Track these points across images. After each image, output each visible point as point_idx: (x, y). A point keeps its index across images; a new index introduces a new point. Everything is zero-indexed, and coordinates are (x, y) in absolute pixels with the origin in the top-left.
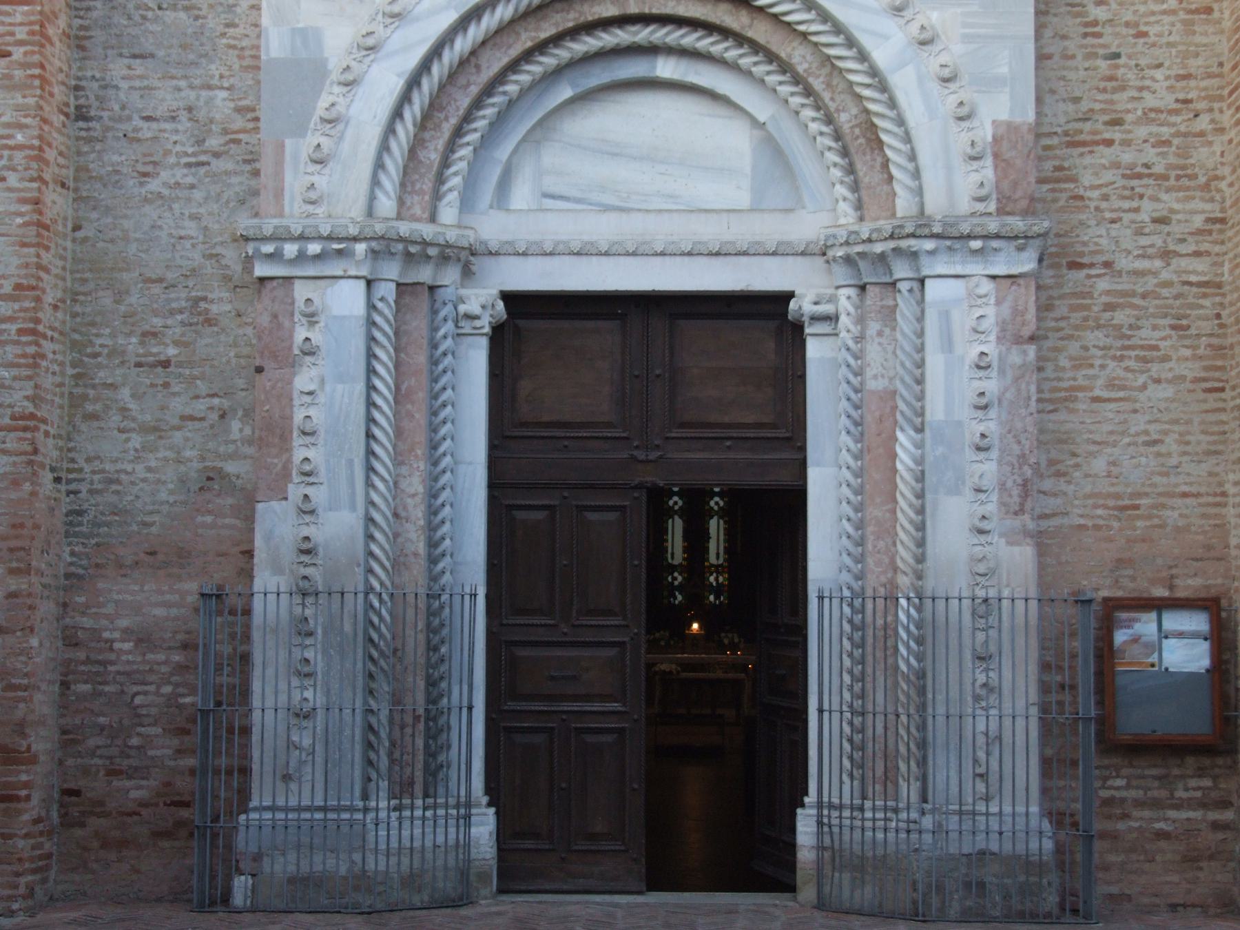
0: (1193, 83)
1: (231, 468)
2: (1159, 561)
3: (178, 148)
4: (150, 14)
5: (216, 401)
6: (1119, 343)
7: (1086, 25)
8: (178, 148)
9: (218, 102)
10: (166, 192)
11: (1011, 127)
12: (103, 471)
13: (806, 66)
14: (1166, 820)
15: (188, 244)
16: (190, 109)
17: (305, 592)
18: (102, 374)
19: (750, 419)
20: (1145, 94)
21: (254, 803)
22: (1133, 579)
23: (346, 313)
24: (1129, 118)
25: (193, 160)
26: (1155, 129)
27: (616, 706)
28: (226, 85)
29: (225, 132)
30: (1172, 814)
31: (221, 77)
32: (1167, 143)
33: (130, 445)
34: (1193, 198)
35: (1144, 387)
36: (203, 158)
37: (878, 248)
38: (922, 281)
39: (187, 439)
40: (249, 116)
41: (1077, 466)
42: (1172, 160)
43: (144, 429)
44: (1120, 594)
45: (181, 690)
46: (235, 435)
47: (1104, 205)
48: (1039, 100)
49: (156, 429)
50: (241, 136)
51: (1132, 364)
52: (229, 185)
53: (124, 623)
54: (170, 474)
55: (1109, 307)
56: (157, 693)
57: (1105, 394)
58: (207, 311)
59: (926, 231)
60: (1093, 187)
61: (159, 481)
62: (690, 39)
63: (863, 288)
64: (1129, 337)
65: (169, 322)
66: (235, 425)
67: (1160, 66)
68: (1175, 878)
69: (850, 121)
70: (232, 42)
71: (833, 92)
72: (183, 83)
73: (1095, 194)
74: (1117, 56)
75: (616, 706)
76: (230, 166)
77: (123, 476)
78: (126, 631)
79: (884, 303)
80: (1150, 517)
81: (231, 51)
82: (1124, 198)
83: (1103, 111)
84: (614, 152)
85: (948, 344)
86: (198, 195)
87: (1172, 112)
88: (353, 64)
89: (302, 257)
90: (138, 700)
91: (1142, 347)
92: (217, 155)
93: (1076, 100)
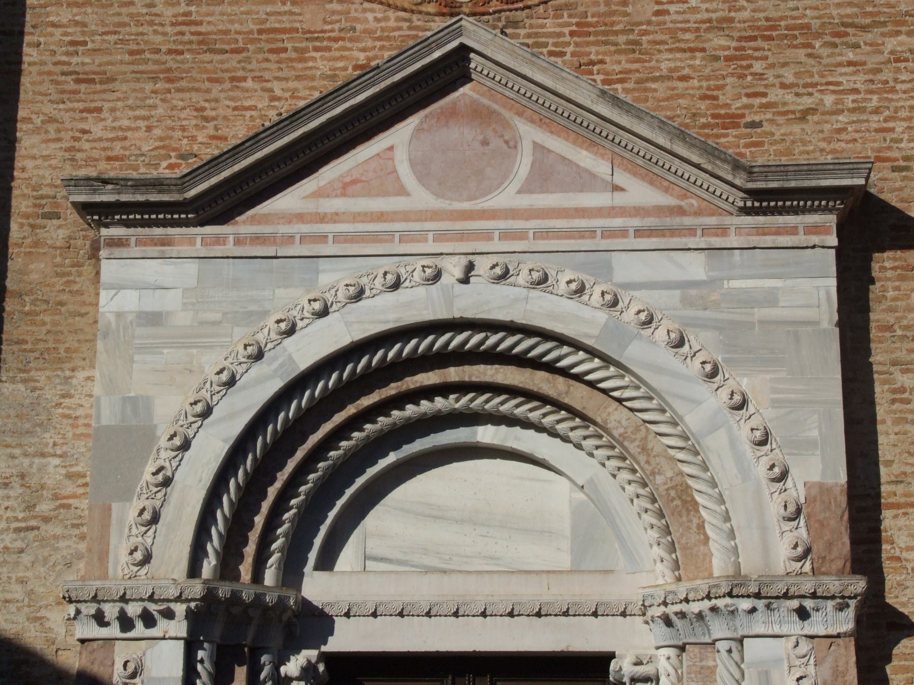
3: (9, 514)
7: (894, 391)
8: (9, 514)
9: (51, 469)
13: (621, 430)
15: (12, 607)
16: (22, 476)
23: (167, 675)
25: (23, 525)
28: (59, 452)
31: (55, 444)
36: (33, 523)
37: (695, 607)
38: (740, 641)
40: (81, 481)
50: (71, 501)
52: (57, 549)
59: (743, 591)
62: (509, 406)
63: (682, 648)
69: (665, 484)
70: (67, 412)
71: (649, 455)
72: (17, 451)
76: (58, 531)
79: (704, 663)
81: (65, 421)
84: (436, 515)
86: (26, 559)
92: (46, 520)
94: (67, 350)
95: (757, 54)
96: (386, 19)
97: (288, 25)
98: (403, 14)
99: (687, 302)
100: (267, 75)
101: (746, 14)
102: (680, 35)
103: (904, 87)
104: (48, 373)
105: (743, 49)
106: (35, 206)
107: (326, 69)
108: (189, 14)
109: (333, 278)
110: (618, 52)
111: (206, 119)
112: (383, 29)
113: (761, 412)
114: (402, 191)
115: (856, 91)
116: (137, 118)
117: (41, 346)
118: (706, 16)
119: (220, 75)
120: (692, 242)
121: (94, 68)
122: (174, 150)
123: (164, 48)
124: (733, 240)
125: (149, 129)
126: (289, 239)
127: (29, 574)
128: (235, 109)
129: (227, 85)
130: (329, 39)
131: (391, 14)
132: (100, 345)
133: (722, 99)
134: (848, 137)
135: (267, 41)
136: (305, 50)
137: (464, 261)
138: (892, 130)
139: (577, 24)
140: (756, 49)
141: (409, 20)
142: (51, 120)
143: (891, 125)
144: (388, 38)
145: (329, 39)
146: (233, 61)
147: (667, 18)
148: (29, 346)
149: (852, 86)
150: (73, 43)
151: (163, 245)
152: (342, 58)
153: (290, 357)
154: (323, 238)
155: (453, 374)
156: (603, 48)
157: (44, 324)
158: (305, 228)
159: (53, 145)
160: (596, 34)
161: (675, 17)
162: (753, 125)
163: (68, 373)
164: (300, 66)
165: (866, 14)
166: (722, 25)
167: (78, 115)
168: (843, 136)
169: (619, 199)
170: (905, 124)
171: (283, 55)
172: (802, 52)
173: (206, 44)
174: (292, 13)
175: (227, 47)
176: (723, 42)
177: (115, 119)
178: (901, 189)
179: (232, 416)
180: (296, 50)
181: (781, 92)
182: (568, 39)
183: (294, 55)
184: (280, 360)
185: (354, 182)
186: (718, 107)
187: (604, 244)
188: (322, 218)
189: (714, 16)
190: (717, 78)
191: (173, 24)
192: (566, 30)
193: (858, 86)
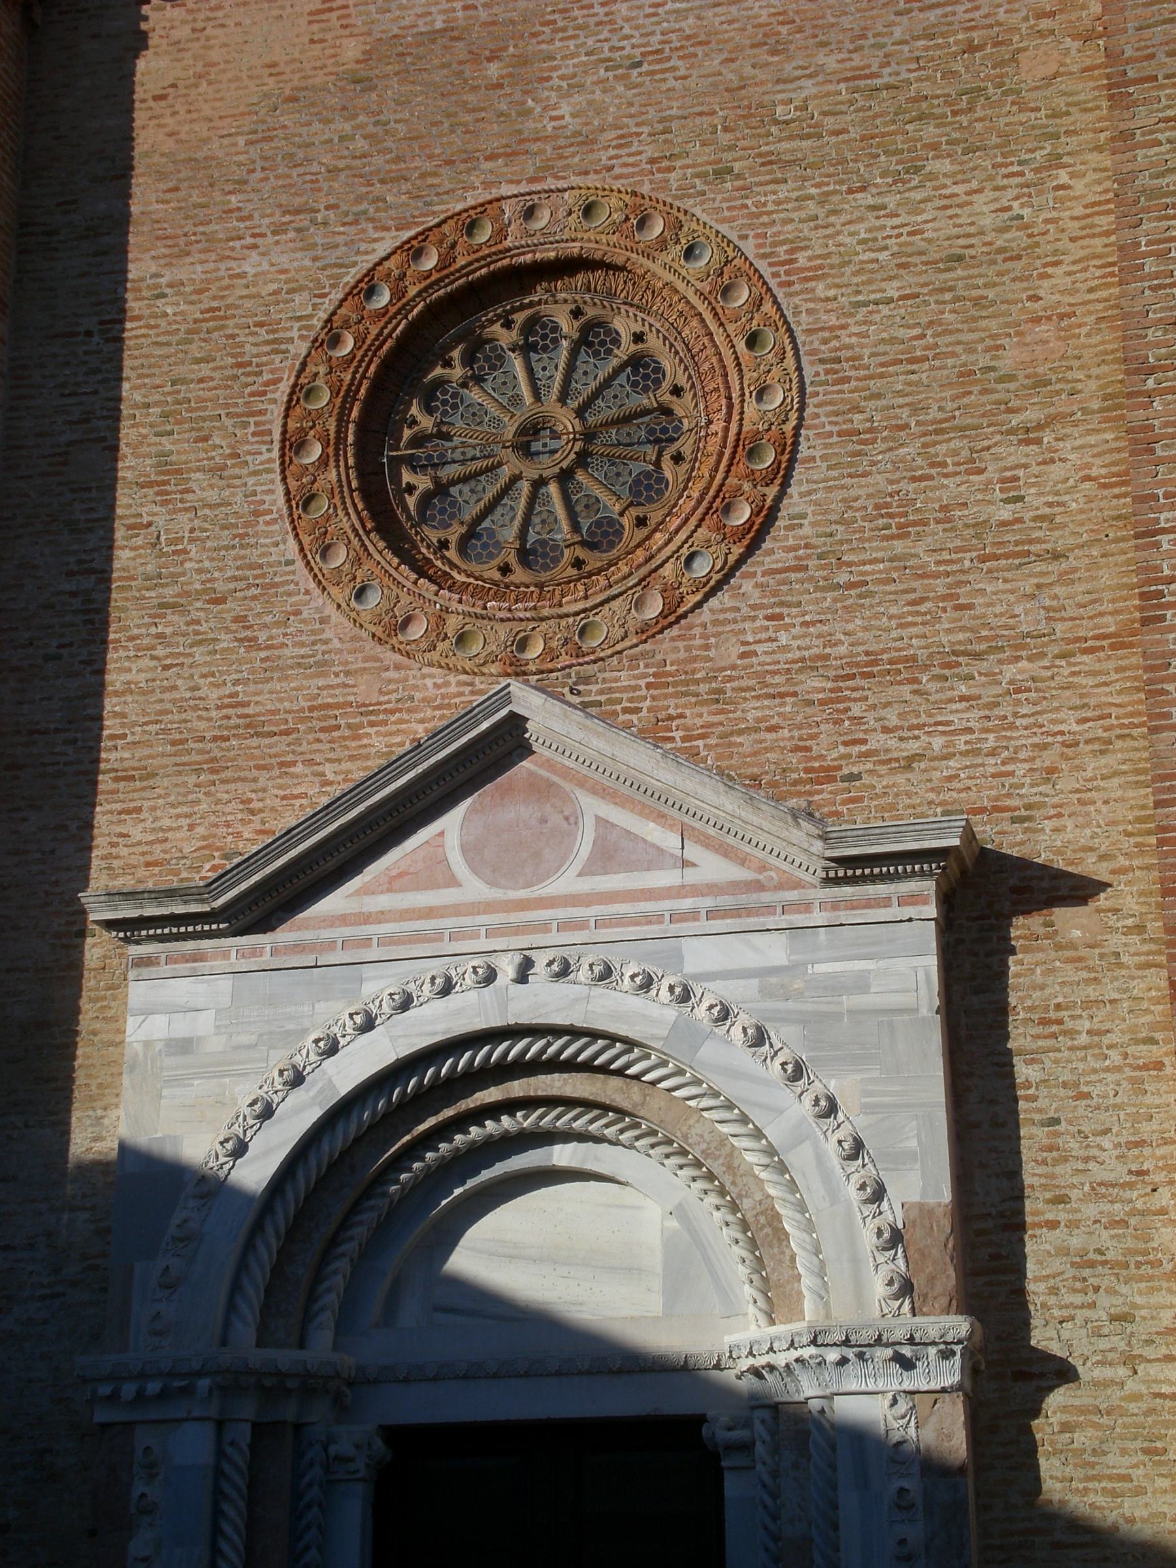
0: (1147, 1151)
6: (1080, 1473)
11: (924, 1212)
20: (1092, 1165)
24: (1074, 1194)
25: (48, 1291)
26: (1107, 1207)
32: (1124, 1223)
34: (1159, 1289)
42: (1130, 1243)
47: (1052, 1300)
55: (1066, 1427)
64: (1092, 1465)
67: (1108, 1131)
71: (735, 1175)
74: (1057, 1121)
82: (1075, 1291)
83: (1044, 1187)
89: (140, 1397)
94: (100, 1086)
95: (855, 695)
96: (447, 684)
98: (464, 677)
99: (766, 992)
100: (318, 758)
101: (843, 649)
102: (769, 679)
103: (1025, 722)
105: (840, 690)
107: (381, 743)
108: (236, 694)
109: (378, 986)
110: (702, 703)
111: (252, 812)
112: (443, 697)
113: (854, 1117)
114: (453, 881)
115: (969, 730)
116: (178, 816)
118: (798, 654)
119: (267, 761)
120: (771, 922)
124: (818, 917)
125: (191, 827)
126: (331, 945)
128: (284, 798)
129: (276, 772)
131: (452, 679)
132: (126, 1080)
134: (960, 786)
135: (318, 719)
136: (360, 726)
137: (518, 958)
138: (1012, 774)
139: (655, 675)
140: (854, 690)
141: (472, 684)
143: (1009, 768)
144: (449, 706)
147: (754, 660)
149: (965, 724)
151: (195, 961)
152: (399, 732)
153: (330, 1081)
154: (366, 942)
155: (517, 1088)
158: (347, 932)
160: (675, 684)
161: (762, 659)
162: (852, 777)
164: (354, 744)
165: (981, 639)
167: (115, 818)
168: (955, 784)
169: (691, 876)
170: (1027, 766)
171: (336, 734)
172: (907, 688)
173: (254, 727)
174: (346, 686)
175: (275, 729)
177: (156, 819)
179: (267, 1153)
181: (882, 737)
182: (644, 692)
183: (347, 733)
184: (319, 1085)
185: (401, 875)
187: (674, 929)
188: (366, 919)
189: (806, 654)
191: (218, 708)
192: (642, 683)
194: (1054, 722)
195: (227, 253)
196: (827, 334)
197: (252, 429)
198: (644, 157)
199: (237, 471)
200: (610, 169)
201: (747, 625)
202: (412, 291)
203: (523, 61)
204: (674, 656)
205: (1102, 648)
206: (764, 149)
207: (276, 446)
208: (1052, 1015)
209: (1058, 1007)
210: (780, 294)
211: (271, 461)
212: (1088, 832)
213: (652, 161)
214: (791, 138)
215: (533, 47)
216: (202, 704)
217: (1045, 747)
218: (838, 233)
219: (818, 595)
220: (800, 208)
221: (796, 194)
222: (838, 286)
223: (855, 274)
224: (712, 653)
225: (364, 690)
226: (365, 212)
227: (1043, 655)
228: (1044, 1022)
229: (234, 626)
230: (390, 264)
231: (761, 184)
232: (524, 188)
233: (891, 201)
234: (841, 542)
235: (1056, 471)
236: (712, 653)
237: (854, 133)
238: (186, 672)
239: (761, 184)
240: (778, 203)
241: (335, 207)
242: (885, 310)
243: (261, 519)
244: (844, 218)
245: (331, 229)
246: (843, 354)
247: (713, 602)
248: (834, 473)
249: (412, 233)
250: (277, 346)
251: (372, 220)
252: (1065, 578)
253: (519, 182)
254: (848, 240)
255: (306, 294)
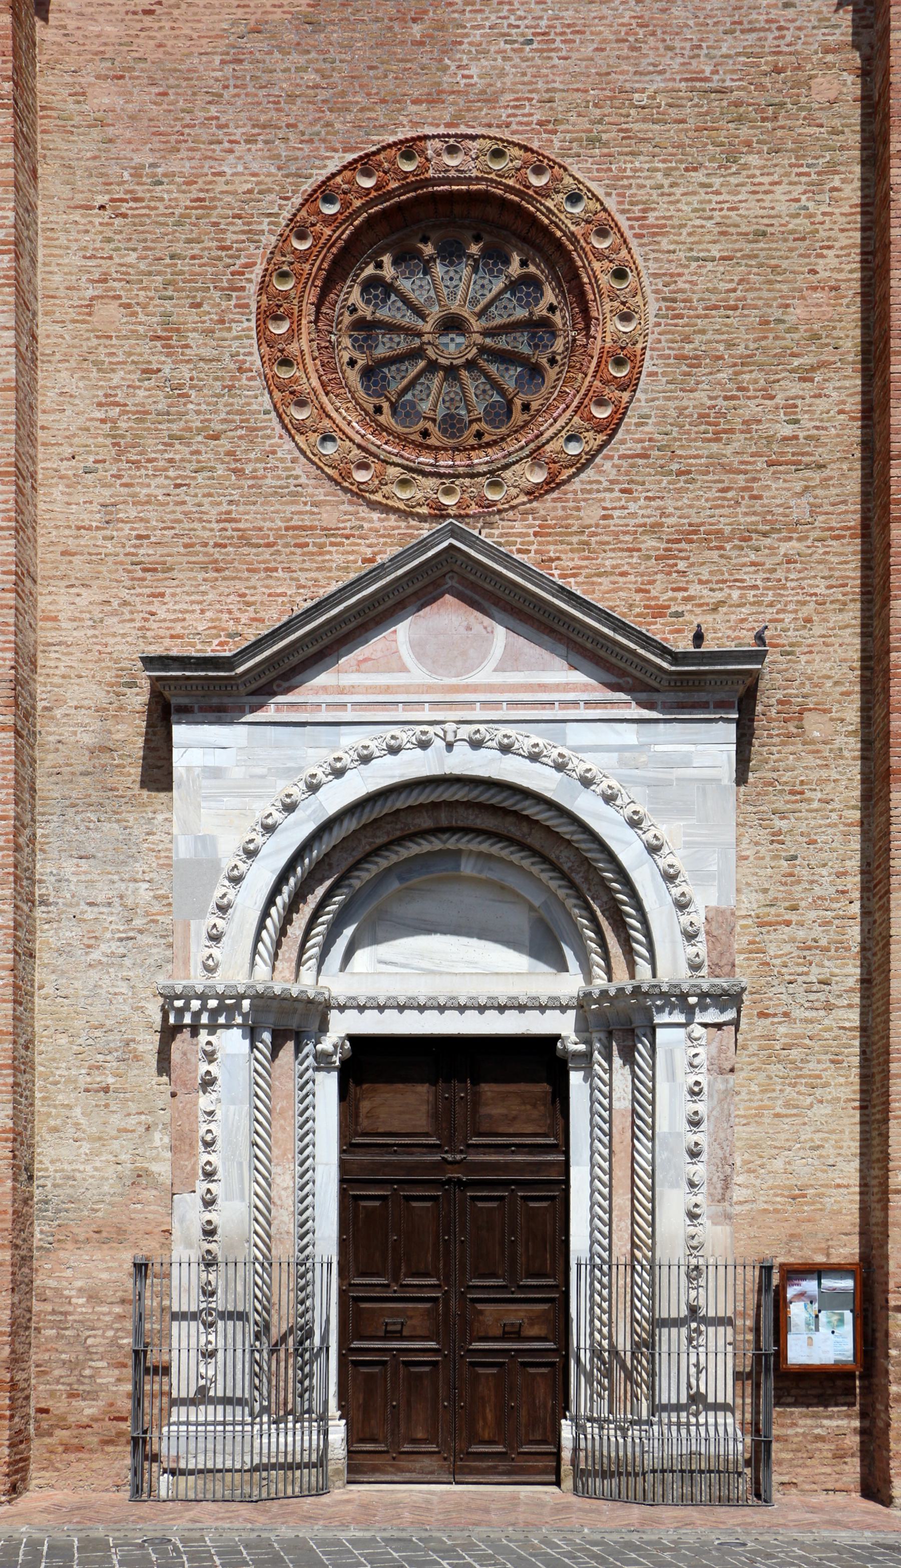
1: (155, 1168)
2: (820, 1235)
3: (113, 926)
4: (92, 825)
5: (143, 1117)
7: (773, 835)
8: (113, 926)
9: (142, 891)
10: (104, 960)
12: (63, 1170)
14: (822, 1426)
15: (120, 999)
17: (209, 1261)
18: (60, 1097)
19: (530, 1129)
21: (174, 1419)
22: (801, 1249)
24: (803, 904)
27: (432, 1345)
29: (147, 914)
30: (826, 1422)
33: (82, 1151)
35: (811, 1105)
36: (131, 934)
39: (122, 1147)
40: (165, 902)
41: (762, 1166)
43: (93, 1139)
44: (792, 1260)
45: (120, 1334)
46: (157, 1143)
47: (784, 970)
48: (738, 891)
49: (100, 1138)
51: (803, 1089)
52: (150, 955)
53: (79, 1284)
54: (110, 1172)
56: (103, 1336)
57: (784, 1111)
58: (135, 1049)
60: (776, 957)
61: (102, 1178)
65: (108, 1058)
66: (157, 1136)
68: (828, 1470)
72: (116, 878)
73: (778, 962)
74: (795, 858)
75: (432, 1345)
76: (151, 940)
77: (78, 1175)
78: (80, 1290)
80: (813, 1203)
82: (798, 964)
83: (785, 899)
85: (672, 1076)
86: (127, 962)
87: (832, 900)
88: (240, 864)
90: (90, 1341)
91: (810, 1076)
92: (141, 932)
93: (765, 891)
95: (682, 554)
97: (308, 523)
100: (294, 566)
102: (622, 538)
103: (793, 584)
104: (136, 815)
105: (669, 550)
106: (117, 676)
108: (229, 512)
110: (572, 551)
111: (248, 604)
112: (385, 528)
115: (755, 587)
116: (192, 602)
117: (129, 793)
118: (641, 521)
119: (256, 566)
121: (156, 558)
122: (223, 630)
123: (211, 543)
125: (203, 611)
127: (131, 973)
128: (270, 595)
129: (263, 574)
130: (342, 536)
133: (654, 593)
135: (293, 537)
138: (782, 620)
139: (540, 526)
140: (680, 551)
142: (125, 603)
143: (781, 616)
145: (342, 536)
146: (266, 554)
147: (611, 522)
148: (120, 793)
150: (139, 537)
152: (352, 552)
156: (559, 547)
157: (130, 775)
159: (128, 625)
160: (557, 534)
161: (617, 521)
163: (150, 815)
164: (320, 558)
165: (765, 522)
166: (654, 528)
167: (146, 600)
174: (313, 513)
176: (654, 543)
178: (786, 670)
180: (315, 544)
181: (699, 587)
183: (315, 549)
186: (649, 599)
189: (648, 521)
190: (649, 575)
192: (531, 531)
193: (759, 583)
194: (811, 586)
195: (209, 154)
196: (667, 279)
197: (233, 302)
198: (535, 119)
199: (225, 334)
200: (508, 125)
201: (607, 495)
202: (358, 203)
203: (441, 26)
204: (552, 514)
205: (844, 537)
206: (624, 126)
207: (253, 317)
208: (798, 788)
209: (802, 783)
210: (633, 243)
211: (249, 329)
212: (828, 665)
213: (540, 123)
214: (644, 120)
215: (444, 14)
216: (205, 517)
217: (804, 603)
218: (678, 201)
219: (658, 477)
220: (650, 178)
221: (647, 166)
222: (677, 243)
223: (690, 234)
224: (582, 514)
225: (328, 517)
226: (318, 134)
227: (806, 538)
228: (792, 793)
229: (227, 459)
230: (339, 179)
231: (620, 154)
232: (442, 130)
233: (717, 181)
234: (675, 439)
235: (822, 404)
236: (582, 514)
237: (691, 123)
238: (192, 491)
239: (620, 154)
240: (635, 170)
241: (294, 126)
242: (710, 266)
243: (244, 376)
244: (682, 190)
245: (291, 144)
246: (679, 296)
247: (583, 476)
248: (672, 387)
249: (355, 156)
250: (252, 236)
251: (324, 141)
252: (825, 483)
253: (438, 126)
254: (685, 208)
255: (273, 197)
